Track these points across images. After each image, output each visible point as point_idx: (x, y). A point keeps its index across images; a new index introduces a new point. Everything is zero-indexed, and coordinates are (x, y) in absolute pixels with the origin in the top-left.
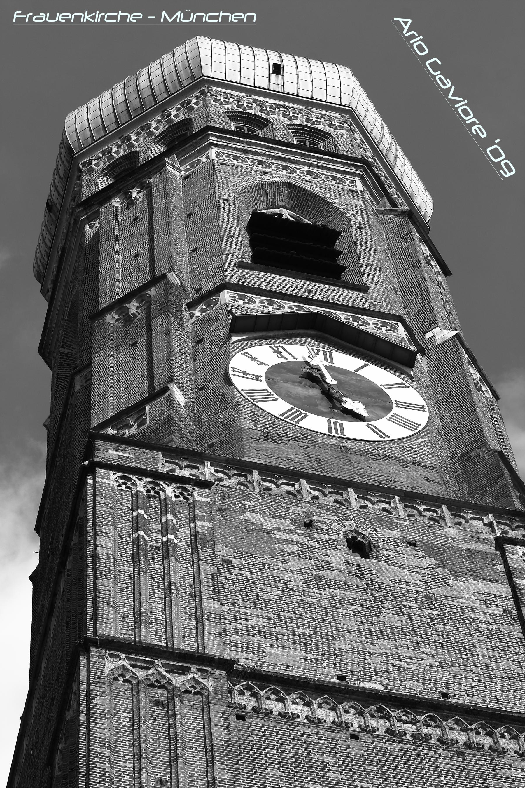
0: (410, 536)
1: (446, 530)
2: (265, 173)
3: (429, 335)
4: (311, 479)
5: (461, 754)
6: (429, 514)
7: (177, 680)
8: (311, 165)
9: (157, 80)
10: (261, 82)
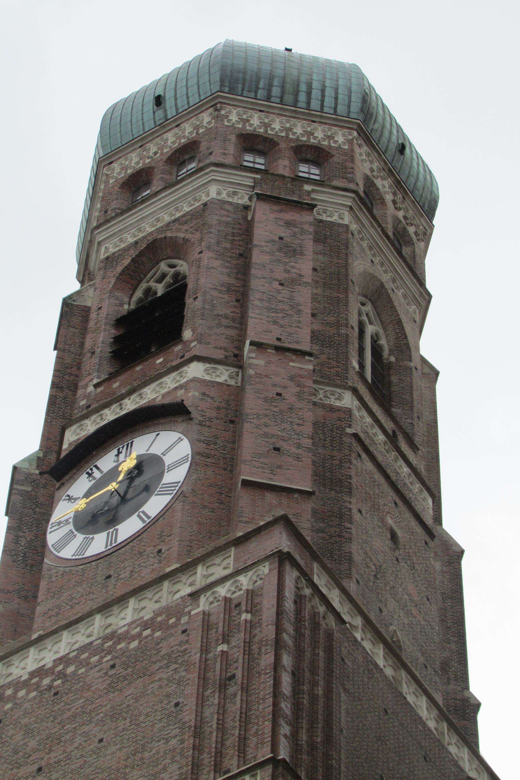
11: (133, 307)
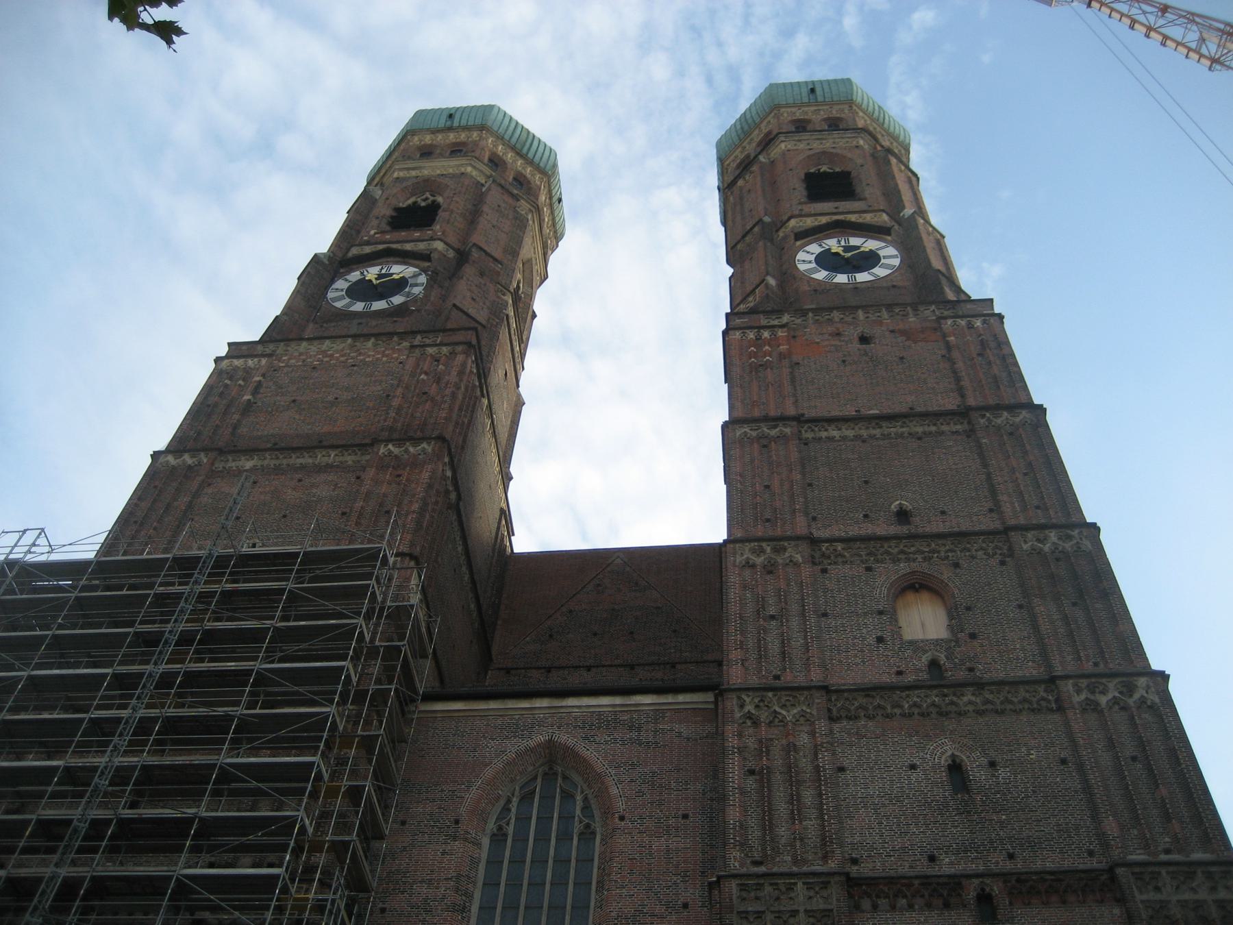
0: (891, 328)
1: (910, 320)
3: (902, 214)
4: (837, 308)
5: (920, 439)
6: (901, 313)
7: (773, 432)
8: (834, 138)
10: (806, 100)
11: (404, 206)
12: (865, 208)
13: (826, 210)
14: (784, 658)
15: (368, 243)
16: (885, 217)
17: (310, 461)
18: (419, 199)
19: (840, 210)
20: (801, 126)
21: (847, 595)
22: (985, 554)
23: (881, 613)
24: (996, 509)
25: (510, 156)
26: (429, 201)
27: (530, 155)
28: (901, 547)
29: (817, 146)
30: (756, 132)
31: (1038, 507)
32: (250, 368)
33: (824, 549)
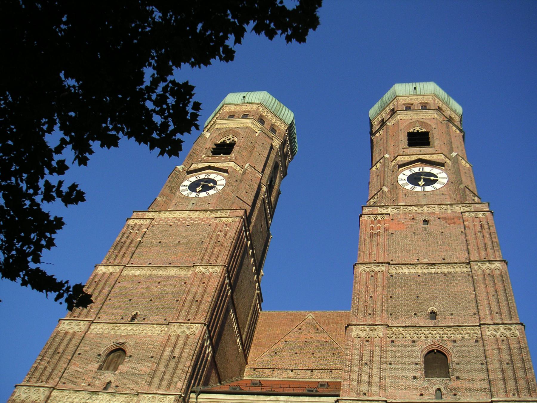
0: (439, 217)
2: (411, 119)
3: (451, 155)
6: (445, 208)
9: (387, 99)
11: (219, 143)
12: (434, 152)
13: (417, 152)
14: (369, 384)
15: (201, 162)
16: (443, 157)
17: (165, 273)
18: (226, 139)
19: (422, 153)
20: (408, 107)
21: (402, 355)
22: (469, 336)
23: (417, 364)
24: (478, 313)
25: (270, 116)
26: (231, 140)
27: (281, 117)
28: (430, 331)
29: (415, 117)
30: (388, 108)
31: (497, 313)
32: (142, 224)
33: (393, 330)
